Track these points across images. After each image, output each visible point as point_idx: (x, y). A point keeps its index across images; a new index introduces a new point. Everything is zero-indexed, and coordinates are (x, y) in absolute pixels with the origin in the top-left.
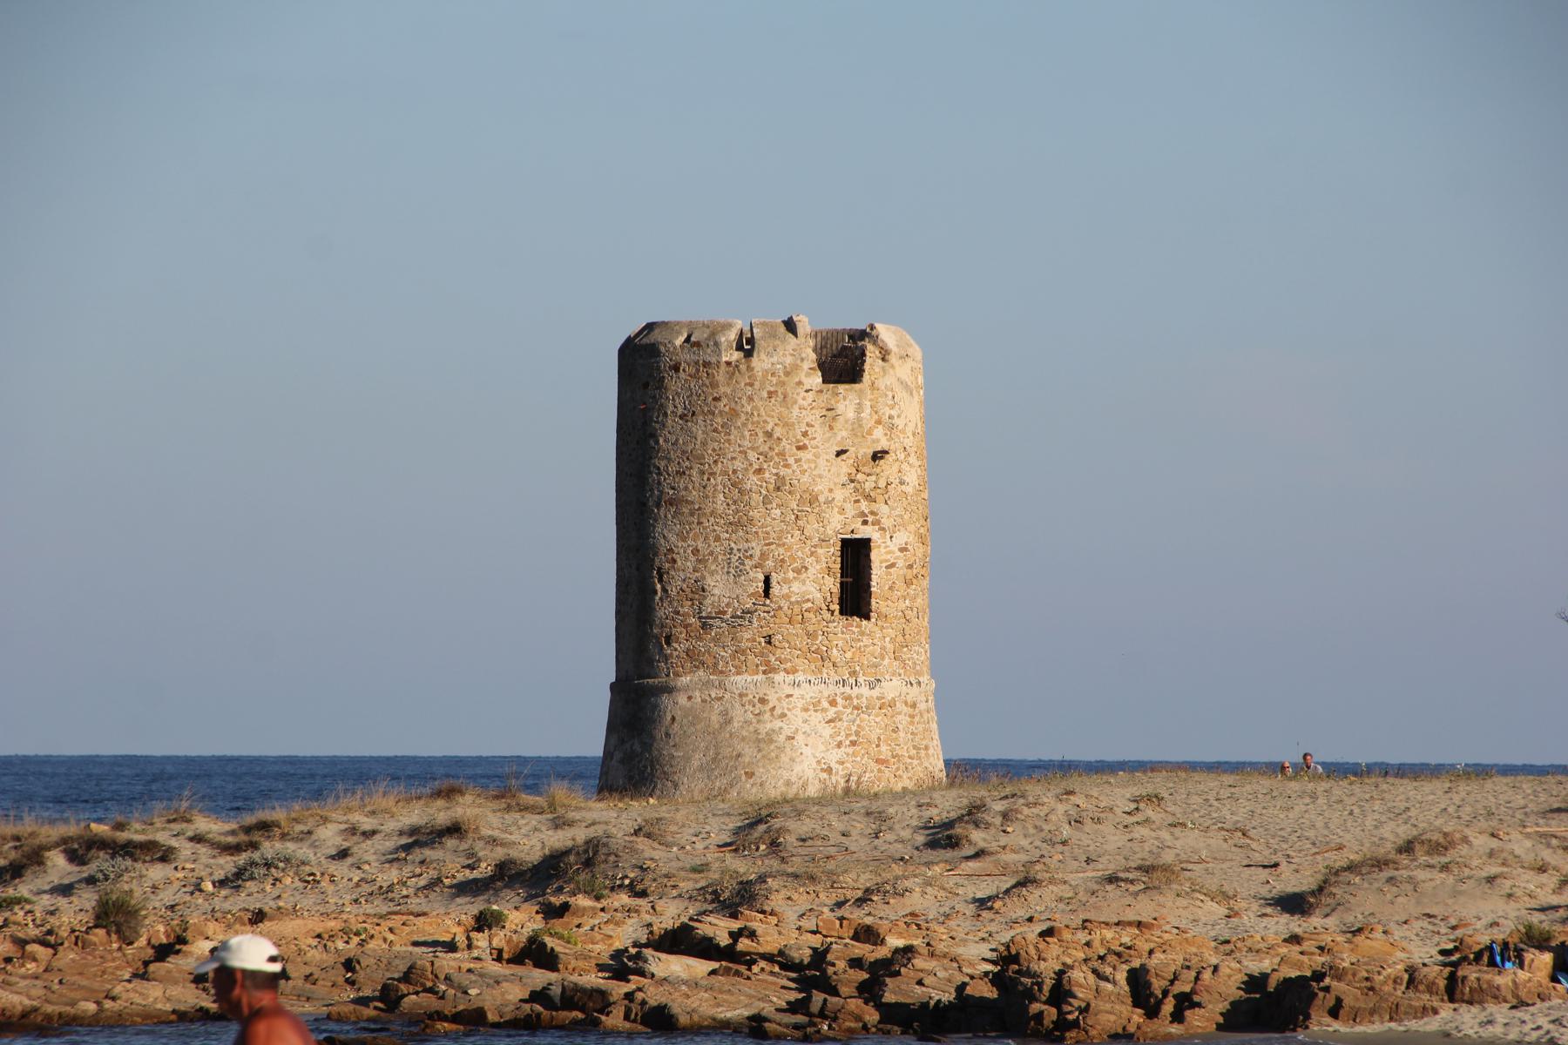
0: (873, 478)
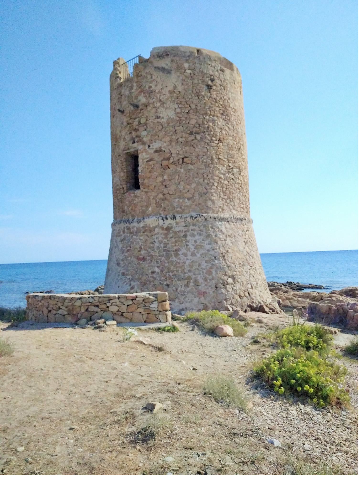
0: (137, 119)
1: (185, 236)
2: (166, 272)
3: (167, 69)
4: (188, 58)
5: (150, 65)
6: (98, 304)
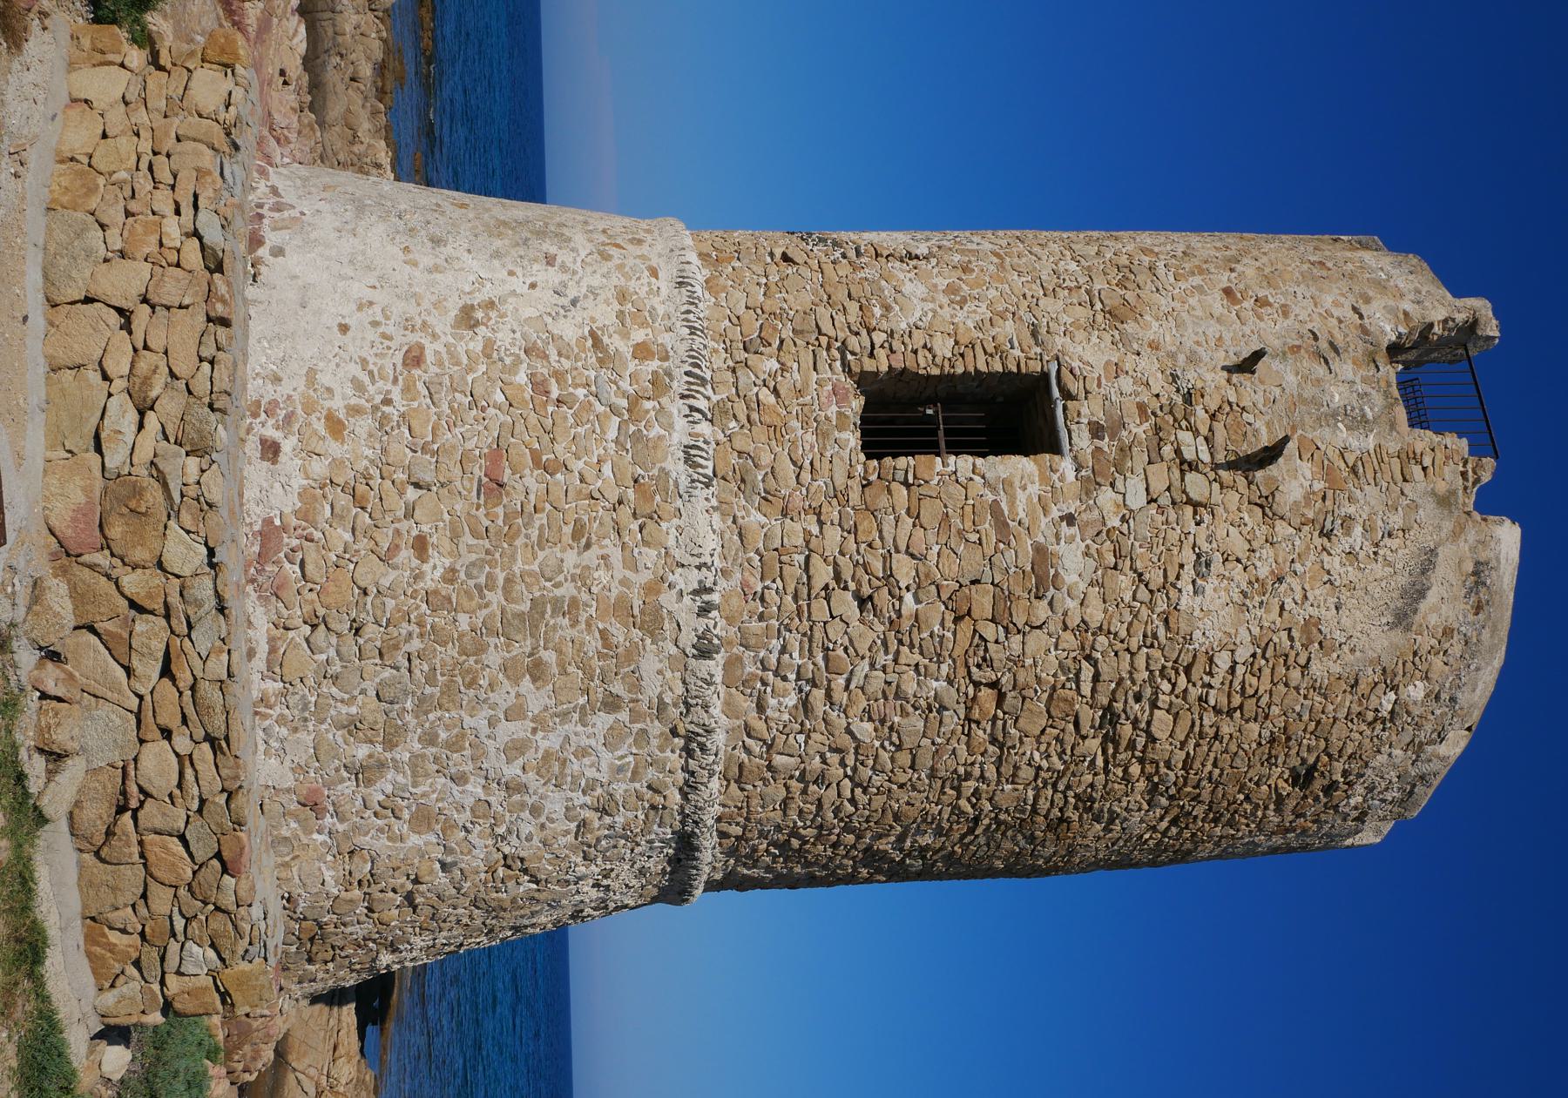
1: (612, 704)
2: (420, 624)
3: (1415, 611)
4: (1445, 696)
5: (1448, 525)
6: (185, 679)
